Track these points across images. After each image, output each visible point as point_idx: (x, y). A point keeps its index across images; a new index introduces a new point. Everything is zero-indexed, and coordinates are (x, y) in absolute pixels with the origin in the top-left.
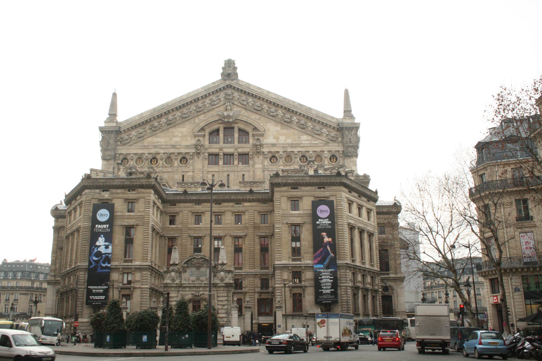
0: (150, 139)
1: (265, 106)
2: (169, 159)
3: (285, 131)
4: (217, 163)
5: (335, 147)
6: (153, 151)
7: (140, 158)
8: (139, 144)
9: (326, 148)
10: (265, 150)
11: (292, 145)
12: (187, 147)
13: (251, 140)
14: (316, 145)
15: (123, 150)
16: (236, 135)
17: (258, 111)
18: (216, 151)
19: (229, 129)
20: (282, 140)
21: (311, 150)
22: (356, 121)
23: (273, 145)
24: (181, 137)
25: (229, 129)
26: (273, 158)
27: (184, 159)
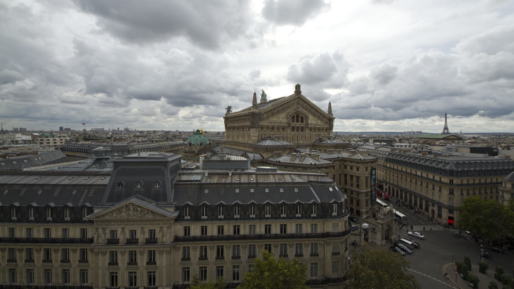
0: (271, 119)
1: (309, 108)
2: (278, 128)
3: (314, 118)
4: (293, 130)
5: (327, 126)
6: (273, 124)
7: (268, 127)
8: (267, 121)
9: (325, 126)
10: (309, 126)
11: (317, 125)
12: (285, 123)
13: (304, 122)
14: (322, 125)
15: (261, 123)
16: (300, 119)
17: (306, 109)
18: (294, 125)
19: (298, 116)
20: (314, 122)
21: (321, 127)
22: (334, 117)
23: (311, 124)
24: (282, 119)
25: (298, 116)
26: (311, 129)
27: (283, 129)
